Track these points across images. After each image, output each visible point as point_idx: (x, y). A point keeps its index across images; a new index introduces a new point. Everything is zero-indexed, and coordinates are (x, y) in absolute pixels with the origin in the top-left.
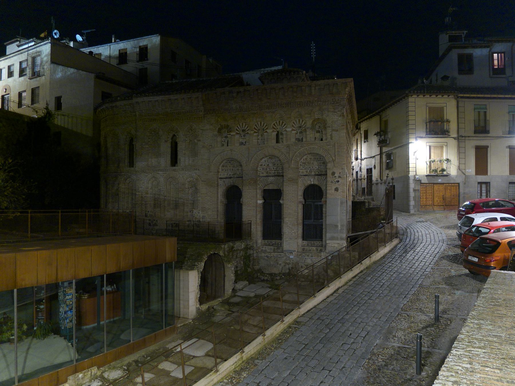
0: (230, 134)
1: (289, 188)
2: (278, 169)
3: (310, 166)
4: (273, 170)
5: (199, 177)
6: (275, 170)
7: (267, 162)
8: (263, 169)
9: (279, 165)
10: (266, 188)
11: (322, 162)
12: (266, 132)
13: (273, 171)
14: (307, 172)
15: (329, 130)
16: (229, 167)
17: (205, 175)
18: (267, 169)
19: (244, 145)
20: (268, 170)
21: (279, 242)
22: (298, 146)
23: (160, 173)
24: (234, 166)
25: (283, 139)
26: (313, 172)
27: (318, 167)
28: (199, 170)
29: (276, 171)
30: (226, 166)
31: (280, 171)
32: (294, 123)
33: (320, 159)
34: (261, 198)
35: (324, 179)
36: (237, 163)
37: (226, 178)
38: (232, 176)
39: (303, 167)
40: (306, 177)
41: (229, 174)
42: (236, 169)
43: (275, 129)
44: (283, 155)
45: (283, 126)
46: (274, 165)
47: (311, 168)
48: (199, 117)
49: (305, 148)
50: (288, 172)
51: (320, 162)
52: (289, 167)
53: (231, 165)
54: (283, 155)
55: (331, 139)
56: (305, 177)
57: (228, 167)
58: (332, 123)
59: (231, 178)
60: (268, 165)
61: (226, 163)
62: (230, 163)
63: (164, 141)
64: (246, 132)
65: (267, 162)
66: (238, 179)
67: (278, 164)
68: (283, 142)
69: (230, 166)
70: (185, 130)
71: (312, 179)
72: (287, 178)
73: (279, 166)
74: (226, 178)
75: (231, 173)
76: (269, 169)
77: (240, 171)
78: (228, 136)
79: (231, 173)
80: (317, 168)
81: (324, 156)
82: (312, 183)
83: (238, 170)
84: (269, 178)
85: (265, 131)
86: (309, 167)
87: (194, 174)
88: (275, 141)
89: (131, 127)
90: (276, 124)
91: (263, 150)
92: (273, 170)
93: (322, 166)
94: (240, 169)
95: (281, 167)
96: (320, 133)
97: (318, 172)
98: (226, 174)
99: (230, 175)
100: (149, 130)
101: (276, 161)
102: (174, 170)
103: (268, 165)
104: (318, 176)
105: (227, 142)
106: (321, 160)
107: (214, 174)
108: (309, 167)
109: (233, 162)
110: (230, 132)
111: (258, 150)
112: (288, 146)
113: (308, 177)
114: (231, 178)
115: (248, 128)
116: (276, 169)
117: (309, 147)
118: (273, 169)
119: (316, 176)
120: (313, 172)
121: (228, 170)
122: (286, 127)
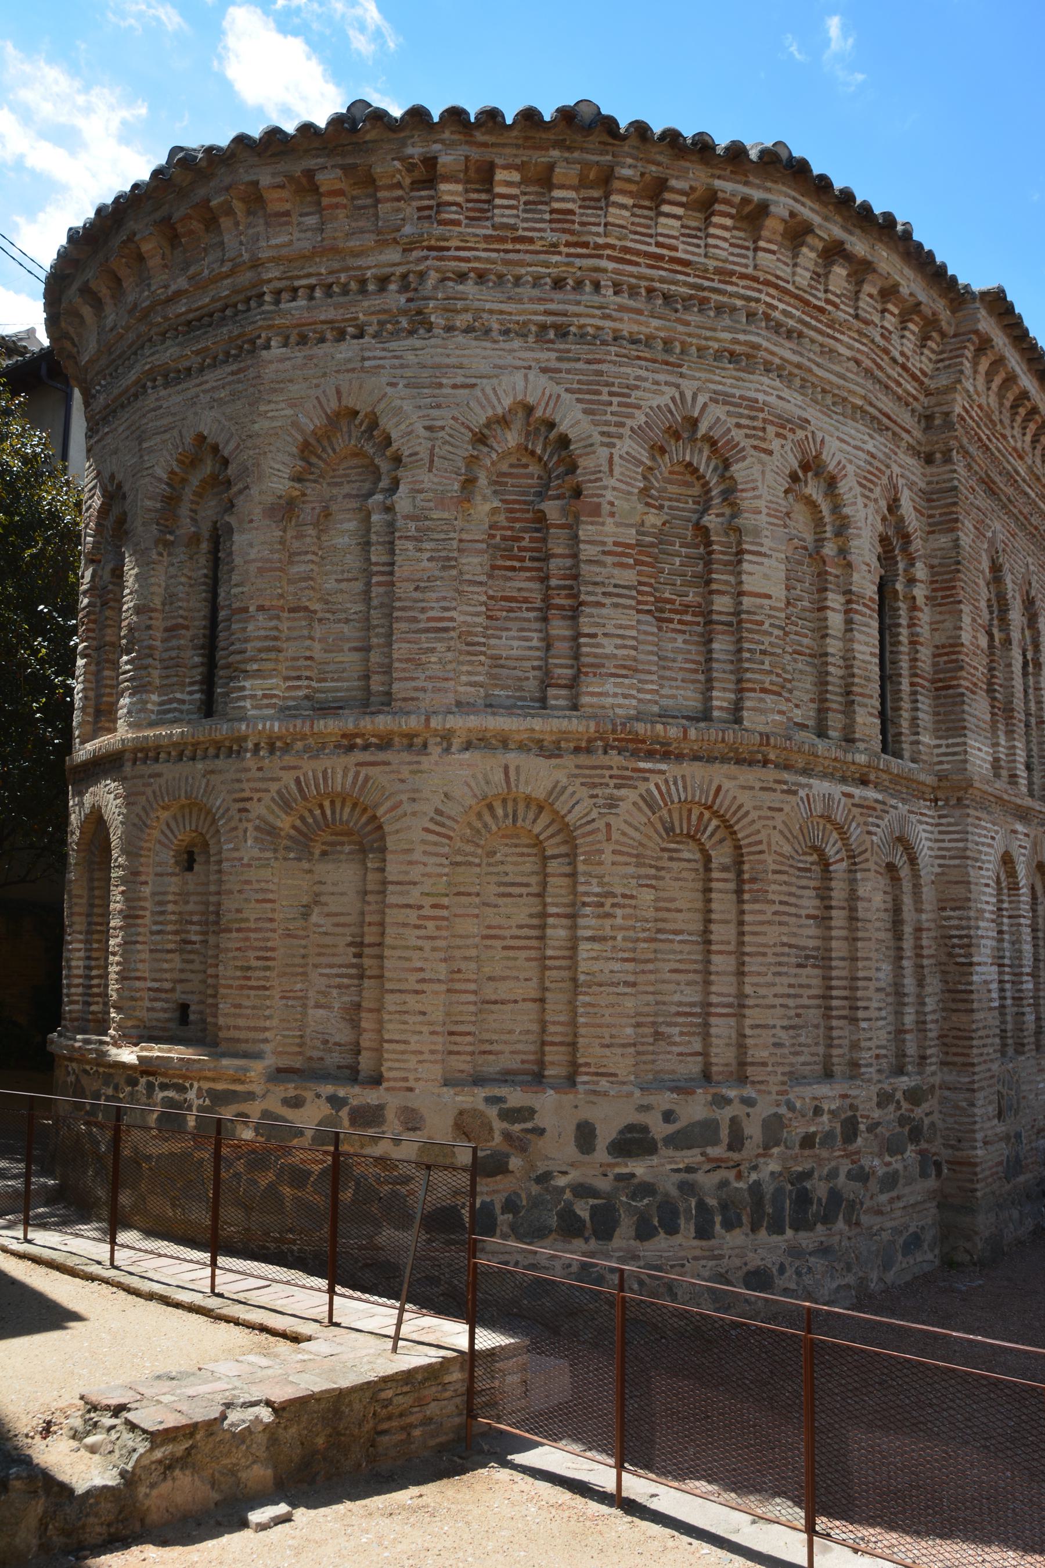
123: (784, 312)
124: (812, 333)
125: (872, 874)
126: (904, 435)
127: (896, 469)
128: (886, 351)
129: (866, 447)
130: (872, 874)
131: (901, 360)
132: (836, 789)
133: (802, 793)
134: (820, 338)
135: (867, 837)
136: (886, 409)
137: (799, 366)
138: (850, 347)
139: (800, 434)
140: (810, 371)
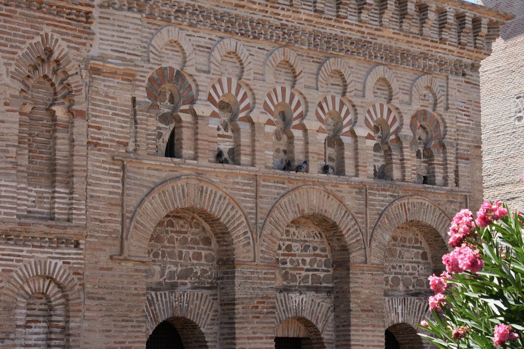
1: (365, 338)
2: (315, 266)
3: (394, 264)
4: (302, 269)
5: (76, 277)
6: (308, 267)
9: (318, 252)
11: (421, 251)
13: (304, 273)
16: (169, 242)
17: (102, 269)
18: (285, 263)
20: (289, 265)
22: (383, 193)
24: (184, 241)
26: (401, 284)
27: (414, 268)
28: (77, 245)
31: (322, 275)
32: (369, 112)
33: (417, 241)
38: (179, 281)
41: (167, 271)
42: (191, 252)
44: (350, 217)
47: (398, 270)
48: (79, 11)
50: (361, 281)
51: (415, 250)
52: (366, 262)
53: (175, 236)
54: (350, 217)
55: (457, 183)
57: (166, 243)
58: (458, 135)
62: (172, 225)
65: (284, 237)
66: (196, 292)
67: (315, 249)
69: (171, 241)
70: (20, 53)
71: (400, 307)
72: (359, 301)
73: (318, 255)
75: (173, 268)
76: (292, 262)
77: (203, 261)
80: (411, 271)
82: (400, 322)
83: (198, 257)
86: (394, 267)
87: (60, 263)
90: (324, 105)
91: (297, 192)
92: (302, 269)
93: (420, 267)
94: (204, 253)
95: (324, 259)
96: (421, 159)
97: (414, 286)
98: (157, 268)
99: (172, 275)
103: (289, 248)
104: (413, 298)
106: (419, 245)
107: (137, 270)
108: (394, 267)
109: (181, 222)
116: (311, 263)
117: (410, 201)
118: (301, 266)
119: (409, 298)
120: (401, 284)
121: (163, 256)
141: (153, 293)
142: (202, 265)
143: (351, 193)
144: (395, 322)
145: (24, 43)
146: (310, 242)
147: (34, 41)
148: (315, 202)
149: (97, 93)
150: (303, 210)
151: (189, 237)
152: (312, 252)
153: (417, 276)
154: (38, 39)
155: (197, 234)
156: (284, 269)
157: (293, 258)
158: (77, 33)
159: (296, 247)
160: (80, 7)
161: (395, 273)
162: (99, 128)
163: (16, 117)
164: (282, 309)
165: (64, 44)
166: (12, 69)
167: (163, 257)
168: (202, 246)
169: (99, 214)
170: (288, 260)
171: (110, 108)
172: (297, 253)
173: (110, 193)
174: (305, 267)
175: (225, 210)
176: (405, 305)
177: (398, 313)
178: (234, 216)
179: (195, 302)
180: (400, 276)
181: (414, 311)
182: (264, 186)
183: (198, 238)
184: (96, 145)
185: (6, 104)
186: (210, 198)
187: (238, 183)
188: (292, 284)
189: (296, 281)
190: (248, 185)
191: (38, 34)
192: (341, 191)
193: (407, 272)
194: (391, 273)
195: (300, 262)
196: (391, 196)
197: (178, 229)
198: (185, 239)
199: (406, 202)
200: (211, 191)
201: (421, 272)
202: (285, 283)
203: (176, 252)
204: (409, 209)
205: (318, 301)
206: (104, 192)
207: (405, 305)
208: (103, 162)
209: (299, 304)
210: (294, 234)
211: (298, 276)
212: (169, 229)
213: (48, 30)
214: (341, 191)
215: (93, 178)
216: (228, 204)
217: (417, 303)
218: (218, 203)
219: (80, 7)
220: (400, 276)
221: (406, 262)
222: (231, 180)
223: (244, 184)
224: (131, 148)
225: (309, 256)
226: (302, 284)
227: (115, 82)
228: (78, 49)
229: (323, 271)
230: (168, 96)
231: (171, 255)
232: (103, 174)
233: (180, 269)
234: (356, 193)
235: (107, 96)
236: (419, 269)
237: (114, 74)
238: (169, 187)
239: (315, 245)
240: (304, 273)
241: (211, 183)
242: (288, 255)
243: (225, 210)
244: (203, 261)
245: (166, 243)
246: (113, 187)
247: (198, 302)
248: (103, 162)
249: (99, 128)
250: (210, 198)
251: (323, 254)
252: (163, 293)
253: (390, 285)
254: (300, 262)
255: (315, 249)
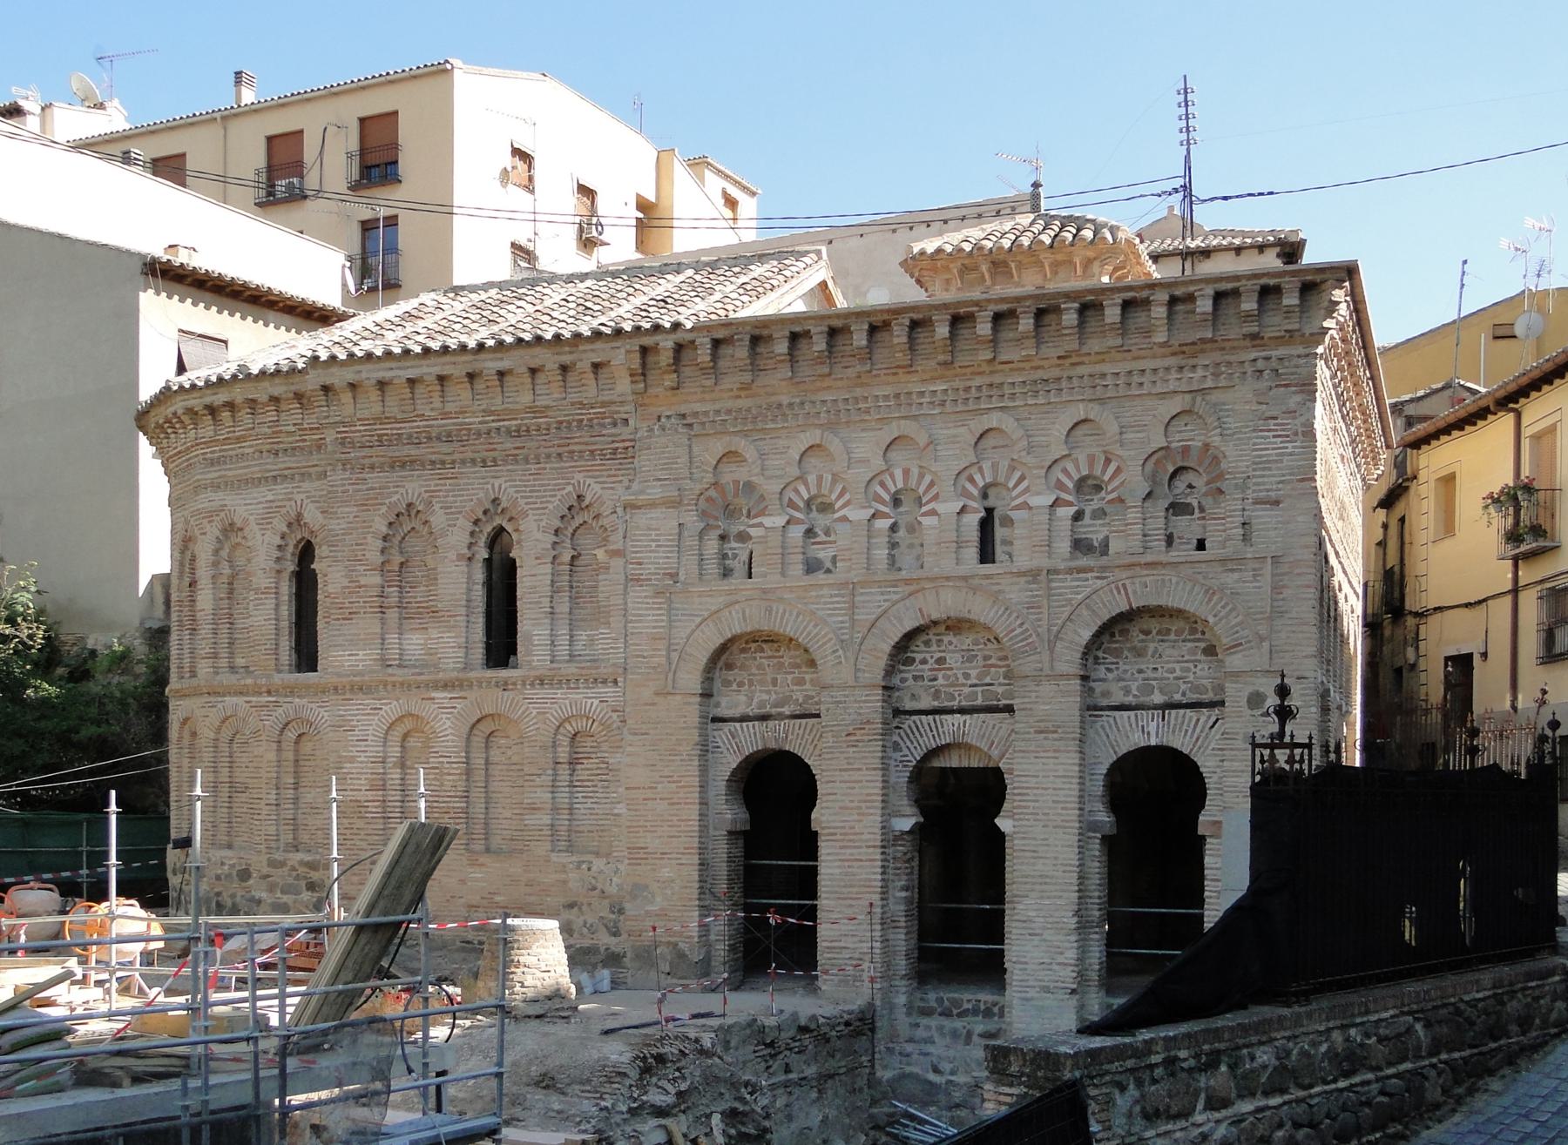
0: (760, 525)
2: (988, 680)
3: (1143, 667)
4: (964, 685)
7: (934, 648)
8: (915, 678)
9: (992, 661)
10: (938, 763)
12: (933, 513)
13: (967, 690)
14: (1127, 692)
15: (1231, 506)
19: (828, 571)
20: (941, 681)
21: (995, 1004)
23: (434, 695)
25: (1011, 543)
27: (1182, 669)
29: (979, 689)
30: (743, 667)
31: (1000, 690)
34: (909, 810)
35: (1210, 723)
36: (792, 653)
37: (744, 719)
39: (1109, 670)
40: (1125, 714)
41: (755, 700)
43: (968, 495)
45: (1016, 486)
46: (970, 660)
48: (617, 449)
49: (1120, 584)
54: (1015, 615)
55: (1246, 538)
56: (1117, 714)
57: (754, 671)
59: (764, 718)
60: (941, 661)
61: (743, 651)
62: (762, 651)
63: (455, 558)
64: (837, 515)
67: (986, 658)
68: (1011, 556)
69: (759, 667)
71: (1152, 727)
74: (744, 719)
75: (765, 697)
76: (946, 677)
78: (753, 532)
79: (765, 697)
80: (1178, 673)
81: (1211, 620)
82: (1153, 742)
83: (800, 682)
84: (944, 717)
85: (924, 509)
86: (1140, 671)
88: (972, 552)
89: (303, 496)
92: (964, 685)
94: (807, 677)
97: (1184, 694)
98: (743, 698)
99: (762, 704)
100: (384, 509)
101: (976, 643)
102: (505, 686)
103: (941, 661)
105: (745, 557)
108: (1140, 671)
110: (762, 513)
111: (896, 597)
112: (1033, 575)
113: (1132, 713)
114: (764, 718)
115: (847, 497)
116: (979, 677)
119: (1174, 712)
121: (751, 683)
122: (1027, 490)
123: (211, 452)
124: (230, 453)
125: (264, 743)
126: (311, 470)
127: (298, 497)
128: (281, 432)
129: (263, 500)
130: (264, 743)
131: (293, 429)
132: (240, 700)
133: (220, 706)
134: (234, 453)
135: (261, 723)
136: (283, 466)
137: (220, 477)
138: (251, 446)
139: (222, 514)
140: (224, 476)
141: (738, 725)
142: (806, 690)
143: (1016, 584)
144: (1142, 744)
145: (555, 496)
146: (979, 650)
147: (564, 492)
148: (949, 602)
149: (638, 528)
150: (929, 616)
151: (787, 661)
152: (981, 663)
153: (1191, 679)
154: (570, 488)
155: (797, 657)
156: (931, 687)
157: (949, 673)
158: (613, 472)
159: (953, 660)
160: (617, 445)
161: (1144, 679)
162: (640, 564)
163: (548, 568)
164: (930, 735)
165: (597, 487)
166: (543, 524)
167: (750, 686)
168: (804, 669)
169: (641, 650)
170: (940, 676)
171: (653, 541)
172: (954, 665)
173: (654, 627)
174: (969, 682)
175: (805, 628)
176: (1163, 719)
177: (1148, 733)
178: (817, 634)
179: (797, 731)
180: (1154, 683)
181: (1185, 727)
182: (862, 594)
183: (798, 661)
184: (638, 580)
185: (537, 558)
186: (782, 618)
187: (822, 596)
188: (946, 704)
189: (955, 699)
190: (836, 596)
191: (569, 484)
192: (998, 584)
193: (1171, 676)
194: (1136, 680)
195: (960, 676)
196: (1098, 578)
197: (770, 653)
198: (781, 665)
199: (1127, 582)
200: (785, 611)
201: (1199, 673)
202: (936, 703)
203: (769, 678)
204: (1135, 592)
205: (992, 723)
206: (648, 627)
207: (1163, 719)
208: (646, 597)
209: (959, 727)
210: (950, 643)
211: (956, 694)
212: (758, 655)
213: (579, 477)
214: (998, 584)
215: (634, 615)
216: (810, 621)
217: (1191, 718)
218: (795, 621)
219: (617, 445)
220: (1154, 683)
221: (1168, 662)
222: (814, 593)
223: (831, 596)
224: (682, 577)
225: (974, 668)
226: (963, 703)
227: (656, 513)
228: (612, 488)
229: (1000, 684)
230: (745, 512)
231: (762, 683)
232: (647, 609)
233: (774, 696)
234: (1028, 582)
235: (649, 529)
236: (1197, 670)
237: (652, 505)
238: (726, 612)
239: (987, 653)
240: (967, 690)
241: (781, 600)
242: (940, 670)
243: (805, 628)
244: (808, 686)
245: (754, 671)
246: (656, 621)
247: (801, 732)
248: (646, 597)
249: (640, 564)
250: (782, 618)
251: (999, 663)
252: (751, 724)
253: (1135, 696)
254: (960, 676)
255: (986, 658)
